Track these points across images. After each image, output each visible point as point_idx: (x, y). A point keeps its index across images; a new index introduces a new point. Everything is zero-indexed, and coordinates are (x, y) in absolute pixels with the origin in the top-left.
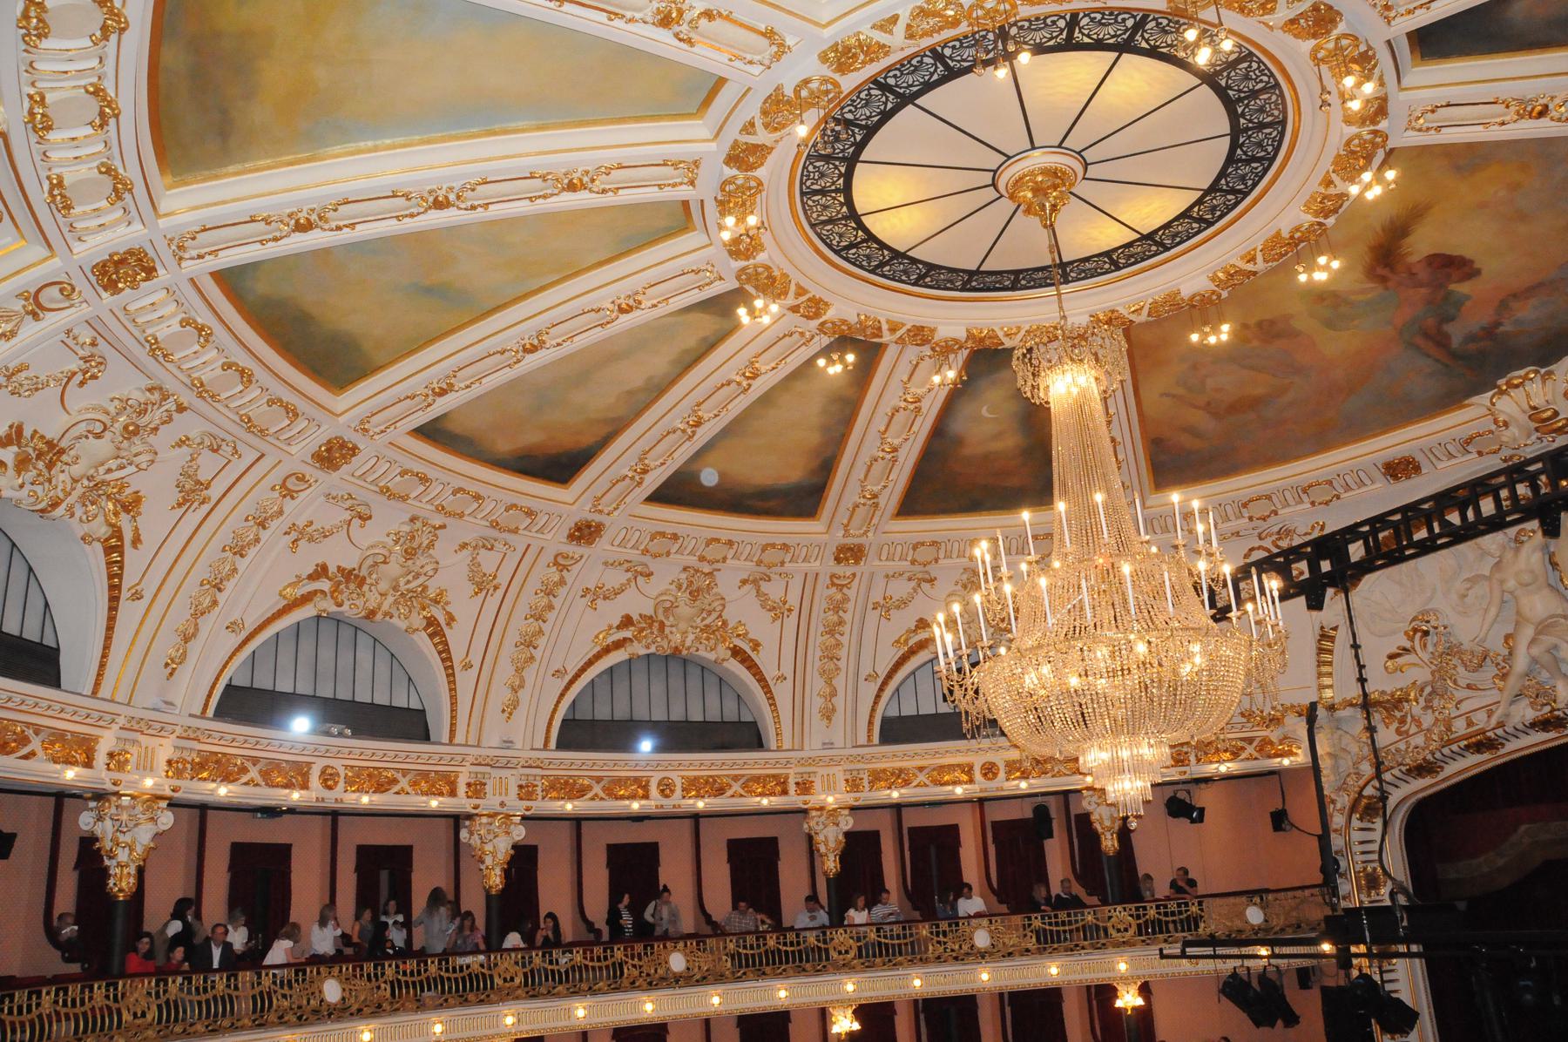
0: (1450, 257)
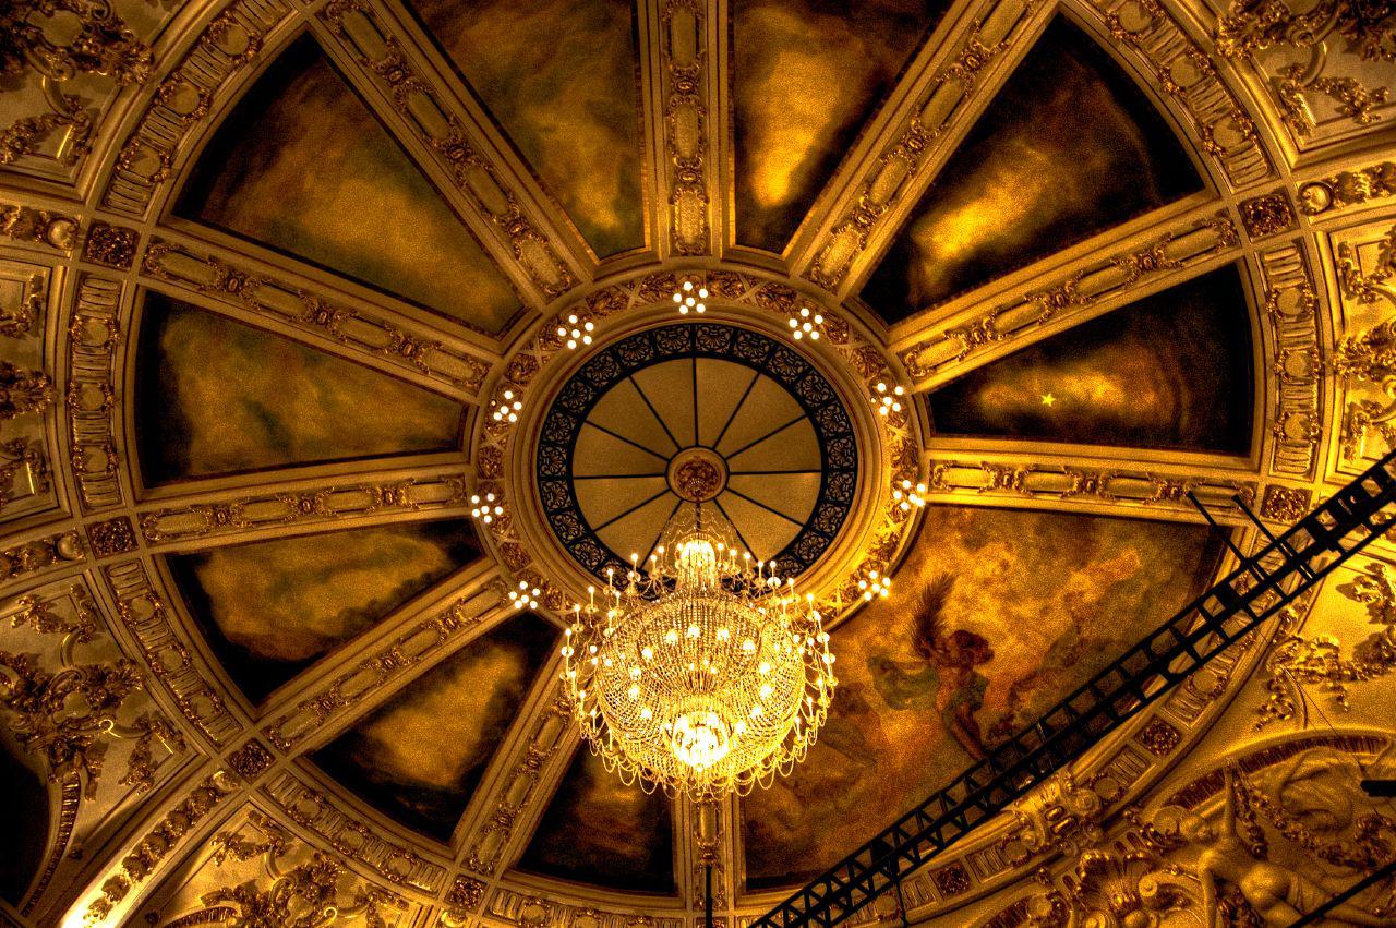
0: (971, 635)
